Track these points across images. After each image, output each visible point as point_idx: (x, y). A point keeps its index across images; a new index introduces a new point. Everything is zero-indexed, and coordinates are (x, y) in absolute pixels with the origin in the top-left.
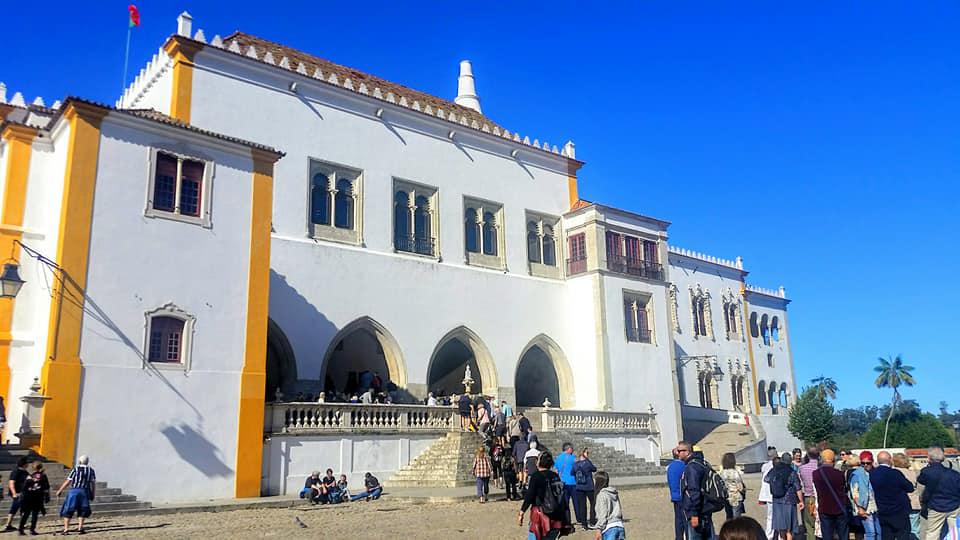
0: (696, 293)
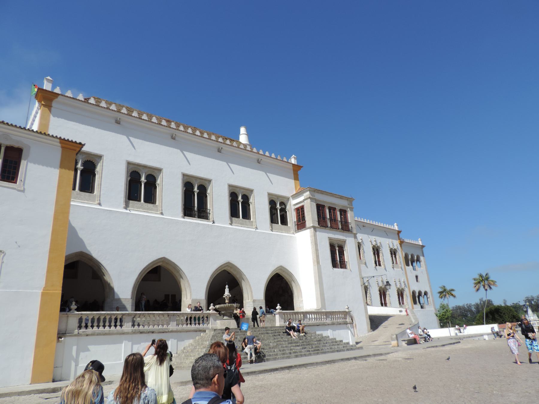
0: (374, 243)
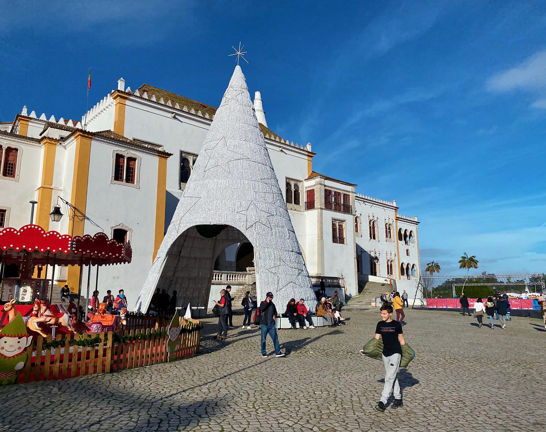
0: (371, 218)
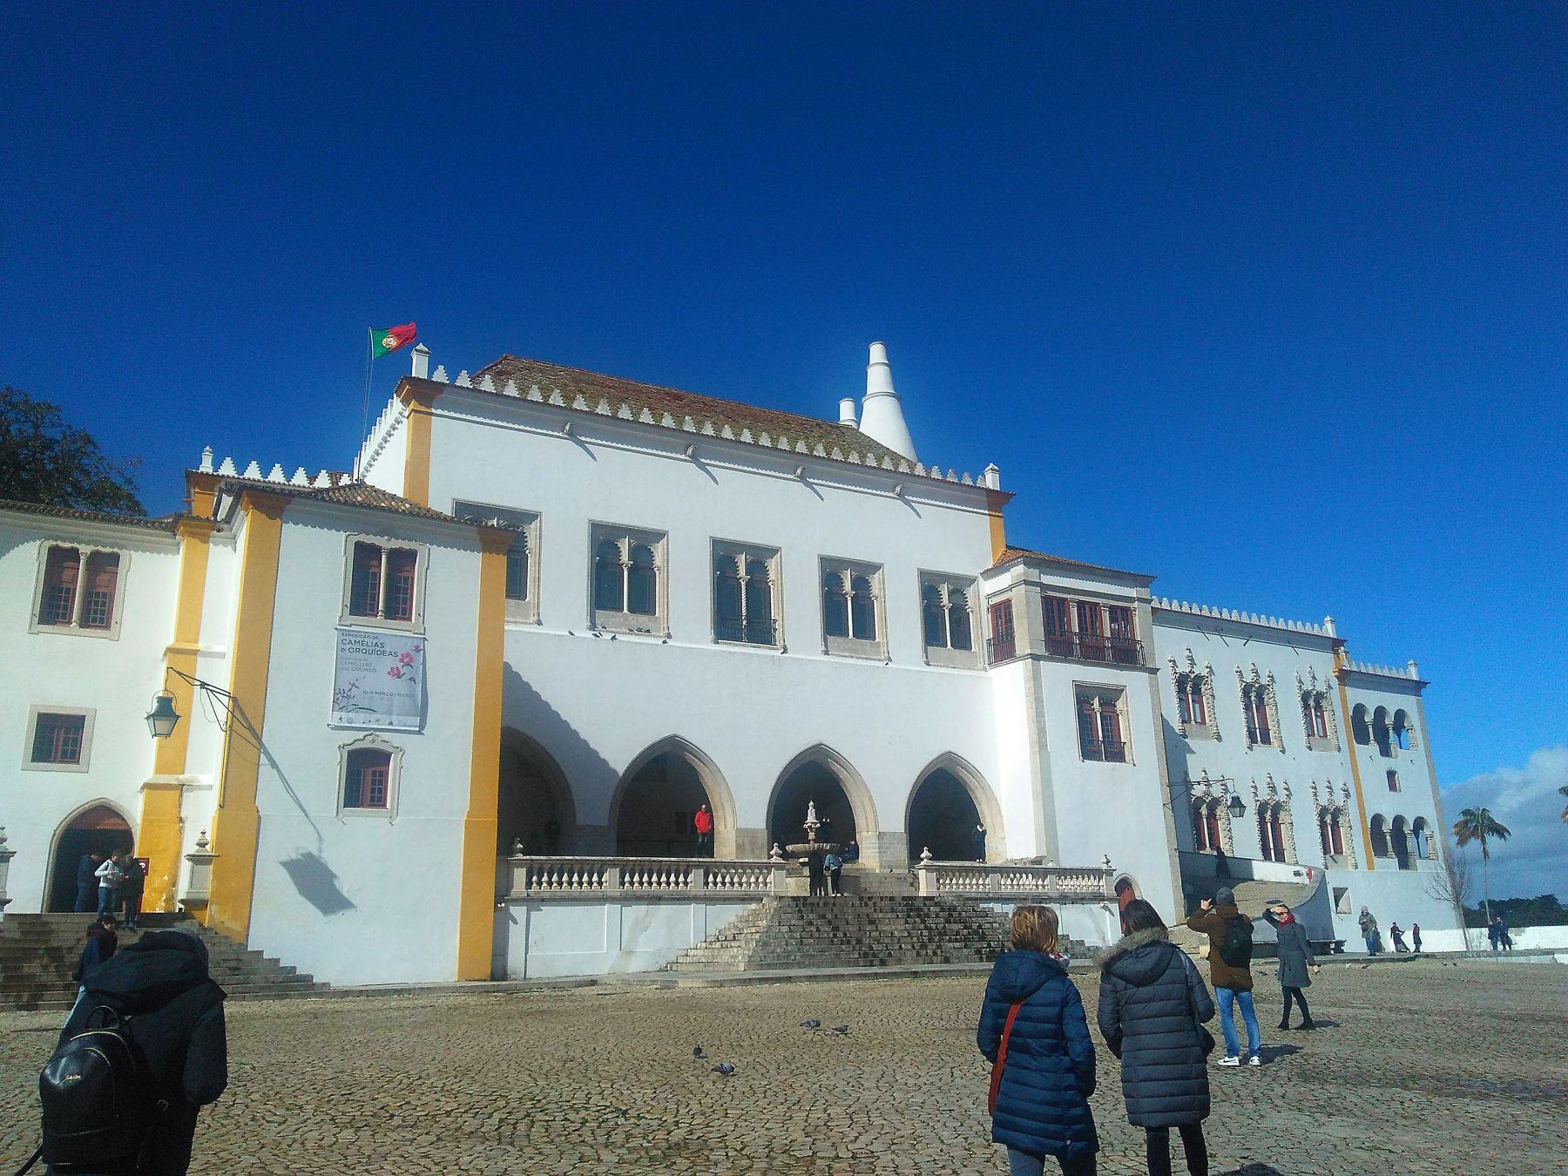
0: (1249, 678)
